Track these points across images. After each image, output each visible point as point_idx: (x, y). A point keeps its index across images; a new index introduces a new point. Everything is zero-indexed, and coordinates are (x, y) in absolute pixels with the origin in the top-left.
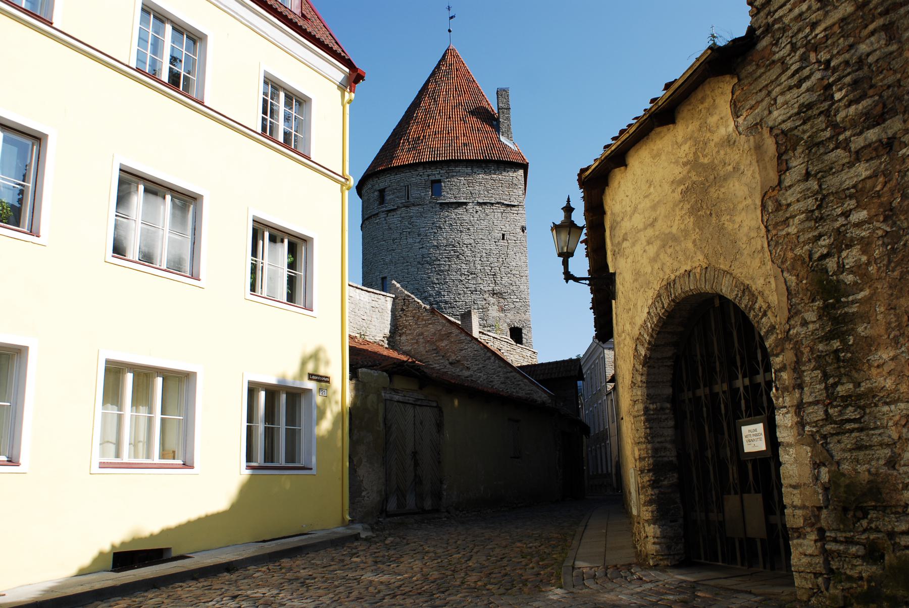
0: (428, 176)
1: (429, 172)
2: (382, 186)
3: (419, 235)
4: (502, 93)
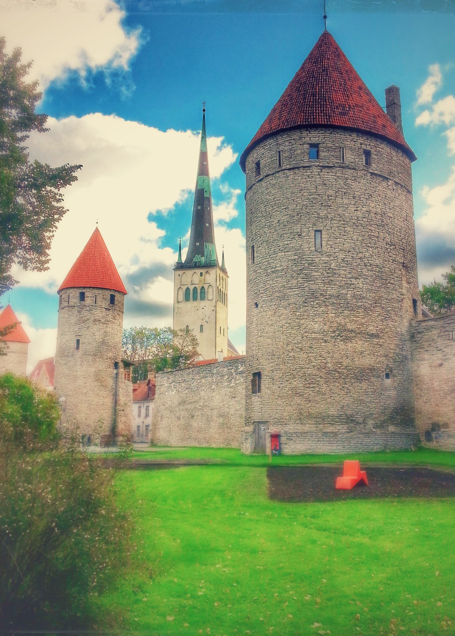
0: (361, 144)
1: (361, 140)
2: (315, 140)
3: (354, 197)
4: (392, 93)
